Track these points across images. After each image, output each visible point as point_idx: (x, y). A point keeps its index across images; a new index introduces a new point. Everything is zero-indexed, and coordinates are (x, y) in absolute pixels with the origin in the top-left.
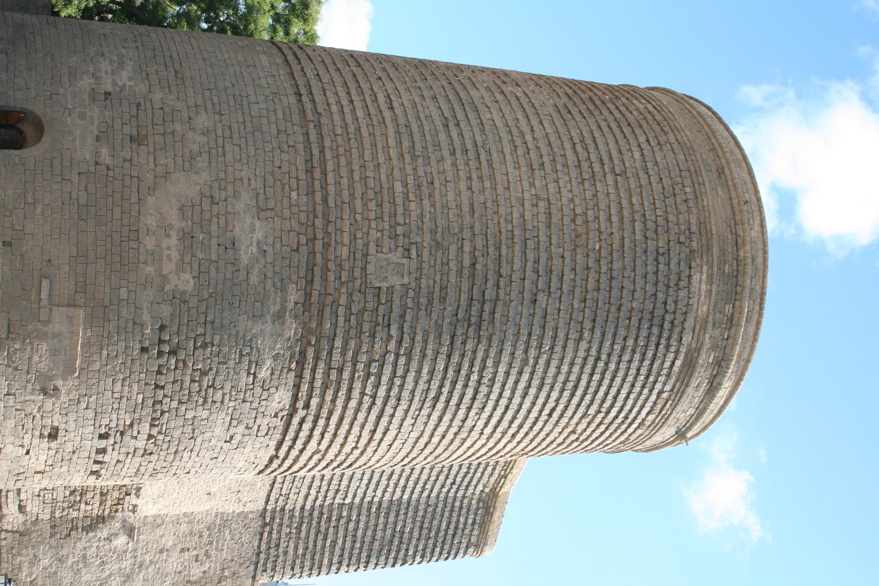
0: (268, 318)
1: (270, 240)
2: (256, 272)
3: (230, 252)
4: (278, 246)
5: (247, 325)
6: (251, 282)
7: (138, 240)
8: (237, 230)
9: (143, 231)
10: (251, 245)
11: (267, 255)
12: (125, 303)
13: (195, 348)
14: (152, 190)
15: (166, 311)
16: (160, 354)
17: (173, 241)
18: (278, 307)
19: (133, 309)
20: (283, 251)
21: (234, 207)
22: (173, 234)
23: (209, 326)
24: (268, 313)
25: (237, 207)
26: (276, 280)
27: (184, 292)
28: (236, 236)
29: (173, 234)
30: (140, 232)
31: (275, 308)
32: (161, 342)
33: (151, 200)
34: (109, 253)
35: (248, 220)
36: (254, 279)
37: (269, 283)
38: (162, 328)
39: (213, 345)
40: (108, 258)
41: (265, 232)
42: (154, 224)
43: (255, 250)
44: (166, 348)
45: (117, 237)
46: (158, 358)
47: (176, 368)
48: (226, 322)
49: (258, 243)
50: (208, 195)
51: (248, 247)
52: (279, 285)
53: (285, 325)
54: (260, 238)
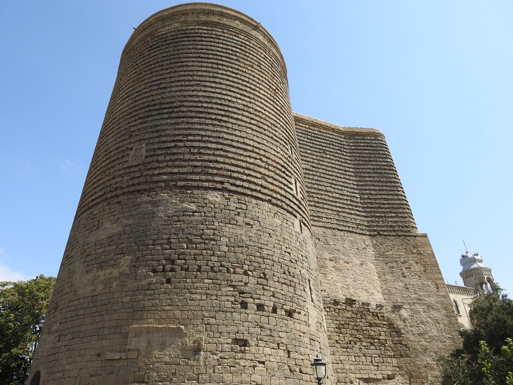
0: (155, 209)
1: (112, 218)
13: (171, 249)
16: (172, 270)
17: (101, 273)
19: (137, 292)
26: (133, 209)
27: (132, 261)
32: (164, 271)
36: (131, 221)
37: (134, 213)
39: (169, 238)
40: (103, 313)
43: (115, 225)
44: (168, 267)
46: (175, 272)
47: (185, 259)
49: (112, 224)
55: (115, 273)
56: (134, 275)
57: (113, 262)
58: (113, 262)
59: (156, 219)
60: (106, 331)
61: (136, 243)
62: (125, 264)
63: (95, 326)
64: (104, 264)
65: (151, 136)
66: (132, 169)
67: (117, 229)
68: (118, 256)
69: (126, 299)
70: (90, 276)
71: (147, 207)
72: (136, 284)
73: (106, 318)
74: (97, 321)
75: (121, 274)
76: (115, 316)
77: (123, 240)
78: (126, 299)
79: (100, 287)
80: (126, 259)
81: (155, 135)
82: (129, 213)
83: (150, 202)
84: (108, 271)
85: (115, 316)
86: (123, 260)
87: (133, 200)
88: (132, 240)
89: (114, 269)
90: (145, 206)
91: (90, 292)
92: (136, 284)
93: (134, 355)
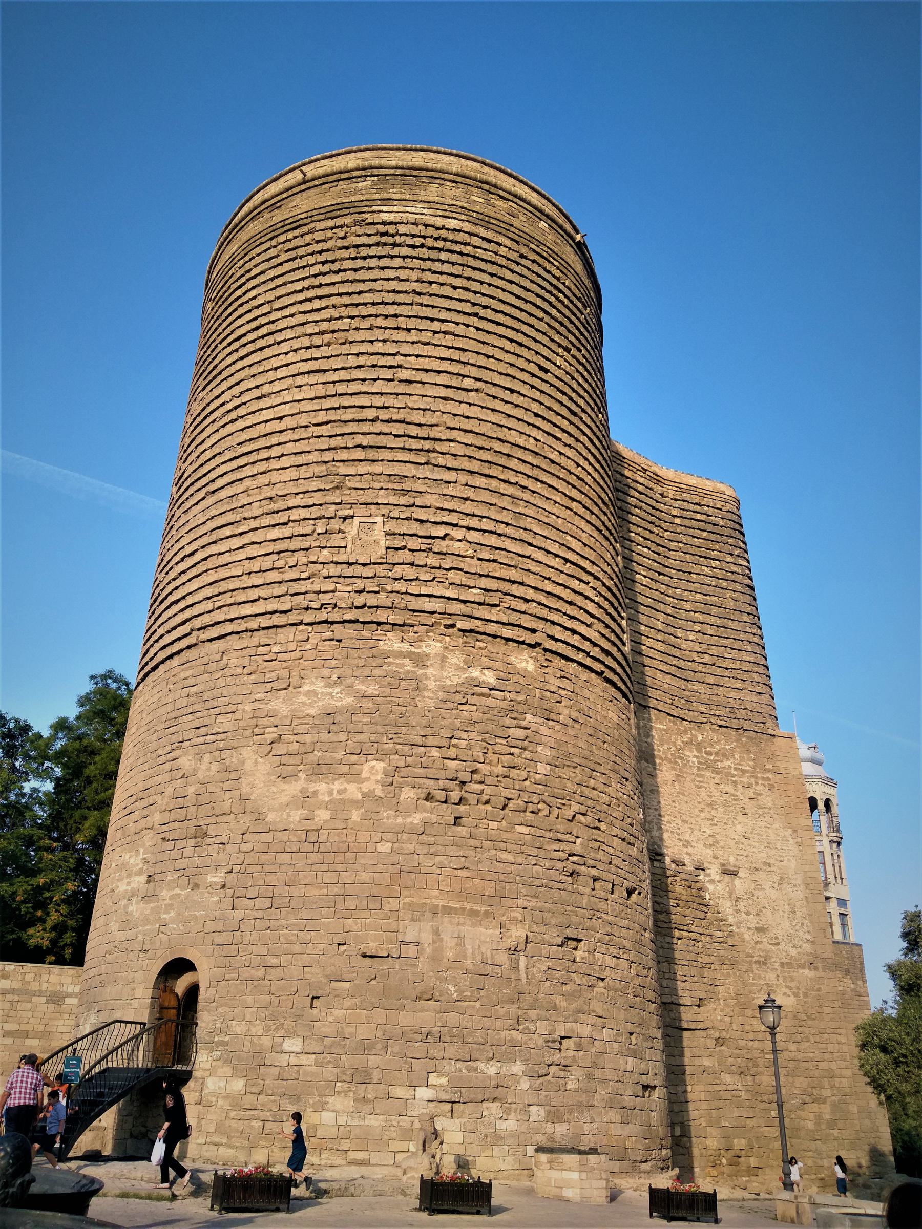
0: (420, 672)
1: (326, 672)
2: (363, 688)
3: (338, 718)
4: (334, 662)
5: (428, 698)
6: (376, 692)
7: (318, 830)
8: (312, 711)
9: (308, 825)
10: (331, 694)
11: (344, 675)
12: (396, 845)
14: (259, 816)
15: (408, 794)
17: (322, 787)
18: (407, 661)
20: (340, 657)
21: (286, 717)
22: (312, 787)
23: (431, 741)
24: (414, 672)
25: (285, 714)
26: (374, 664)
27: (385, 773)
28: (319, 712)
29: (312, 787)
30: (309, 828)
31: (409, 665)
33: (271, 817)
34: (332, 867)
35: (302, 698)
36: (372, 689)
37: (378, 672)
38: (429, 797)
40: (339, 868)
41: (316, 678)
42: (299, 812)
43: (337, 690)
45: (314, 858)
48: (424, 722)
49: (328, 685)
50: (269, 747)
51: (333, 697)
52: (379, 661)
53: (430, 654)
54: (322, 684)
55: (353, 791)
56: (394, 801)
57: (345, 769)
58: (345, 769)
59: (426, 694)
60: (351, 904)
61: (390, 736)
62: (372, 778)
63: (325, 891)
64: (324, 769)
65: (392, 500)
66: (358, 570)
67: (341, 699)
68: (354, 758)
69: (385, 848)
70: (292, 789)
71: (403, 665)
72: (400, 820)
73: (346, 877)
74: (327, 880)
75: (365, 795)
76: (364, 876)
77: (360, 726)
78: (385, 848)
79: (323, 815)
80: (373, 767)
81: (403, 500)
82: (367, 673)
83: (409, 655)
84: (337, 786)
85: (364, 876)
86: (366, 767)
87: (371, 643)
88: (380, 729)
89: (349, 782)
90: (398, 661)
91: (299, 822)
92: (400, 820)
93: (412, 951)
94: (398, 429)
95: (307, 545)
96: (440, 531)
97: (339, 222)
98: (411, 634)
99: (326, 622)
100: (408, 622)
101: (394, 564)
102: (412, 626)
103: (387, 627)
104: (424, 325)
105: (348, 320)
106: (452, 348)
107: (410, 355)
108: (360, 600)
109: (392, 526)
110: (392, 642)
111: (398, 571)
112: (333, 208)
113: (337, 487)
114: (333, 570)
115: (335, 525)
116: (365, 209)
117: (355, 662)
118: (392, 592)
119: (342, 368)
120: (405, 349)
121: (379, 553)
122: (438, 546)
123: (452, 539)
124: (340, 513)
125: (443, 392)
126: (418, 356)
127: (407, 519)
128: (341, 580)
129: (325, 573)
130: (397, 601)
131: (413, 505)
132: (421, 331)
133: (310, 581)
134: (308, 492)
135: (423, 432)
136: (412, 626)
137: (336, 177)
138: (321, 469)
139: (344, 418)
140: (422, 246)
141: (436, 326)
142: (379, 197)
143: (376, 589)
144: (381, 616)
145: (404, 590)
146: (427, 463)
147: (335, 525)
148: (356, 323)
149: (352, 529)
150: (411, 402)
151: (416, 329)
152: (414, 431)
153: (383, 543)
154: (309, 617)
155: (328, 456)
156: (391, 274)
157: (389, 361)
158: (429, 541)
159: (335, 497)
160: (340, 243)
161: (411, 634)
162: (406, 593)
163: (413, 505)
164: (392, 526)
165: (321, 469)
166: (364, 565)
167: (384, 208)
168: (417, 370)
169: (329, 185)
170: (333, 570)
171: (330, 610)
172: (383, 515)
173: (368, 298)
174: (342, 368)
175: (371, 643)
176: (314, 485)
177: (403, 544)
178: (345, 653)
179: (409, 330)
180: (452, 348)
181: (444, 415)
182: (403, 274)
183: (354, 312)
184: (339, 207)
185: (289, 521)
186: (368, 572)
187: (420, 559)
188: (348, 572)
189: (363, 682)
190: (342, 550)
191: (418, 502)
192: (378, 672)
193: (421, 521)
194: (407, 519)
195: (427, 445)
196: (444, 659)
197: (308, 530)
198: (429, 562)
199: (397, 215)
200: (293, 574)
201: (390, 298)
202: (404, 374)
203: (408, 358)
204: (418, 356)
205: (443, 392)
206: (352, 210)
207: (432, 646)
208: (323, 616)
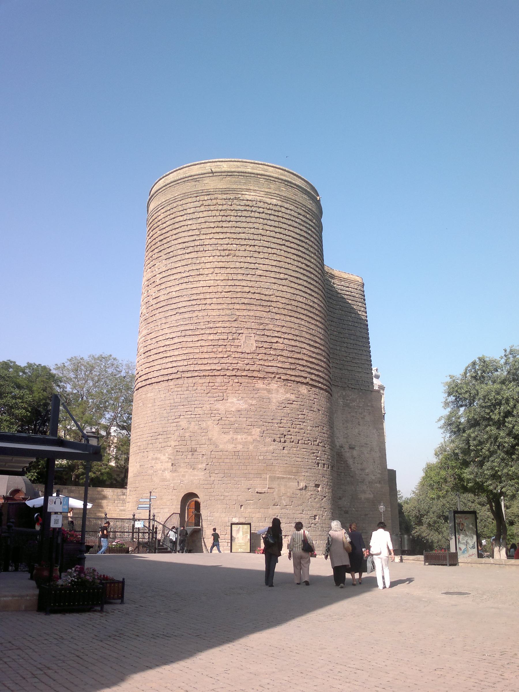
0: (270, 396)
6: (256, 403)
18: (265, 392)
24: (268, 396)
26: (254, 393)
81: (261, 327)
87: (253, 385)
94: (257, 296)
95: (225, 344)
96: (275, 340)
97: (228, 196)
98: (266, 381)
99: (235, 376)
100: (265, 376)
101: (259, 354)
102: (266, 378)
103: (258, 378)
104: (266, 250)
105: (235, 246)
106: (276, 260)
107: (260, 264)
108: (247, 368)
109: (257, 338)
110: (260, 384)
111: (260, 357)
112: (225, 190)
113: (235, 320)
114: (237, 355)
115: (235, 336)
116: (239, 192)
117: (247, 392)
118: (259, 365)
119: (235, 268)
120: (259, 261)
121: (254, 349)
122: (275, 346)
123: (279, 343)
124: (237, 332)
125: (274, 281)
126: (264, 264)
127: (263, 335)
128: (240, 359)
129: (233, 356)
130: (261, 369)
131: (264, 329)
132: (264, 253)
133: (228, 358)
134: (224, 321)
135: (267, 298)
136: (266, 378)
137: (226, 174)
138: (228, 312)
139: (236, 290)
140: (263, 213)
141: (270, 250)
142: (245, 188)
143: (253, 363)
144: (255, 374)
145: (263, 364)
146: (269, 312)
147: (235, 336)
148: (239, 247)
149: (243, 338)
150: (262, 284)
151: (262, 252)
152: (264, 297)
153: (255, 345)
154: (228, 373)
155: (231, 306)
156: (251, 225)
157: (252, 266)
158: (271, 344)
159: (235, 324)
160: (229, 207)
161: (266, 381)
162: (264, 365)
163: (264, 329)
164: (257, 338)
165: (228, 312)
166: (248, 353)
167: (246, 193)
168: (263, 270)
169: (222, 177)
170: (237, 355)
171: (236, 371)
172: (254, 333)
173: (243, 236)
174: (235, 268)
175: (253, 385)
176: (226, 319)
177: (262, 345)
178: (243, 388)
179: (259, 252)
180: (276, 260)
181: (274, 291)
182: (256, 225)
183: (238, 242)
184: (228, 190)
185: (217, 333)
186: (250, 356)
187: (268, 351)
188: (242, 356)
189: (250, 399)
190: (239, 347)
191: (267, 328)
192: (256, 396)
193: (268, 336)
194: (263, 335)
195: (269, 304)
196: (278, 391)
197: (225, 337)
198: (272, 352)
199: (252, 197)
200: (221, 355)
201: (251, 237)
202: (259, 272)
203: (260, 265)
204: (264, 264)
205: (274, 281)
206: (233, 192)
207: (274, 386)
208: (234, 373)
